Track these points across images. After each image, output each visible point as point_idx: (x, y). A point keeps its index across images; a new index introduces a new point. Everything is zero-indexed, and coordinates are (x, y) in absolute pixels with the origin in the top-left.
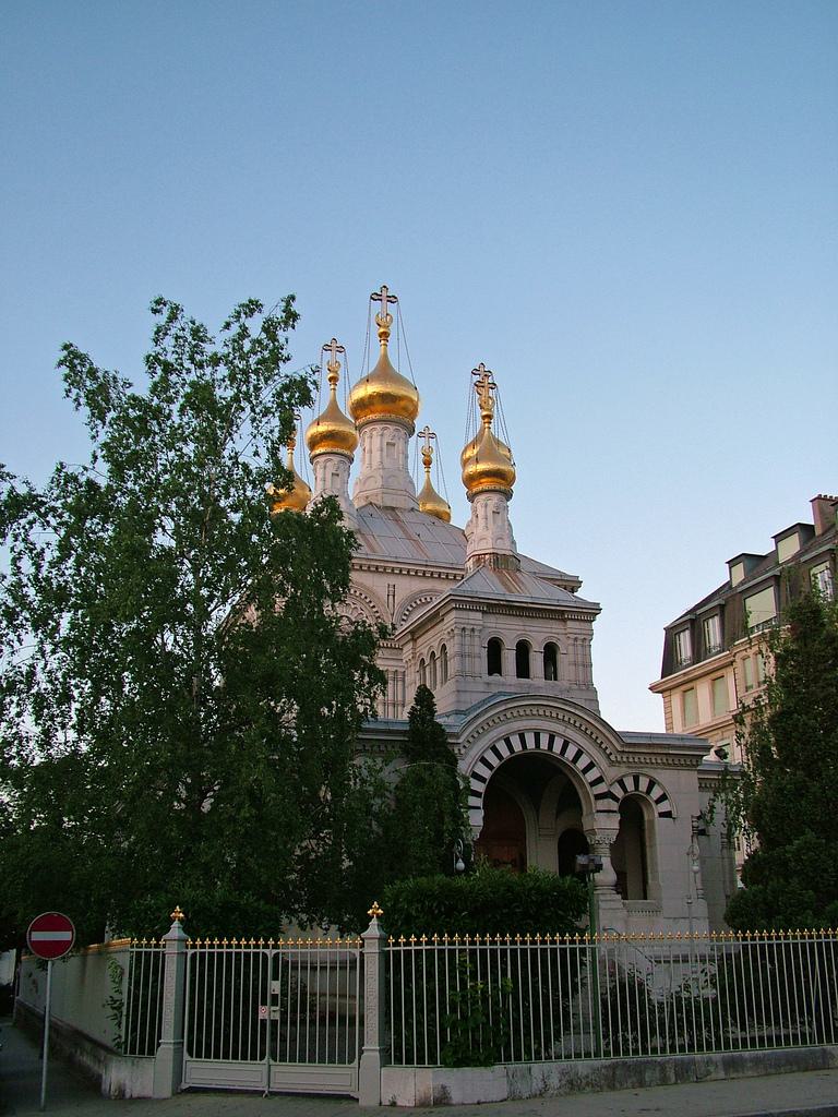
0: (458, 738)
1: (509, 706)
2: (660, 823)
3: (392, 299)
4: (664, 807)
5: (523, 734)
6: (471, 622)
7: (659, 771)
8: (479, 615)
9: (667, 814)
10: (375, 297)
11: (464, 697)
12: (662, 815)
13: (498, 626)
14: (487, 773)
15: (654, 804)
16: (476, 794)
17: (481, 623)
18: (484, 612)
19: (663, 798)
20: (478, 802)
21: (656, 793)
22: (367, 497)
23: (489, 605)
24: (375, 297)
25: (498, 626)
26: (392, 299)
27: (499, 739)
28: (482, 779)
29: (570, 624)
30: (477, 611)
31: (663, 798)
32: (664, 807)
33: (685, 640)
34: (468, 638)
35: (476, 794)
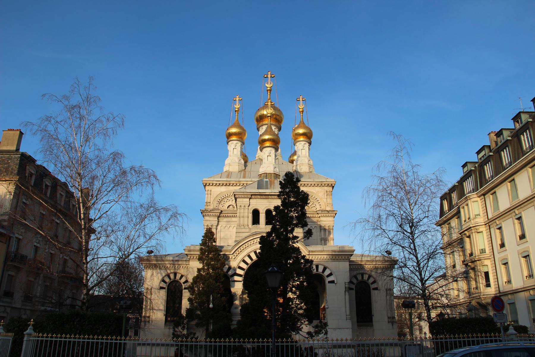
0: (230, 251)
1: (254, 237)
2: (328, 286)
4: (331, 278)
6: (244, 203)
7: (329, 262)
9: (332, 282)
11: (239, 234)
12: (330, 282)
13: (257, 203)
14: (245, 266)
15: (326, 277)
16: (240, 275)
19: (331, 274)
20: (240, 279)
21: (327, 272)
25: (257, 203)
28: (242, 269)
31: (331, 274)
32: (331, 278)
33: (445, 203)
34: (242, 210)
35: (240, 275)
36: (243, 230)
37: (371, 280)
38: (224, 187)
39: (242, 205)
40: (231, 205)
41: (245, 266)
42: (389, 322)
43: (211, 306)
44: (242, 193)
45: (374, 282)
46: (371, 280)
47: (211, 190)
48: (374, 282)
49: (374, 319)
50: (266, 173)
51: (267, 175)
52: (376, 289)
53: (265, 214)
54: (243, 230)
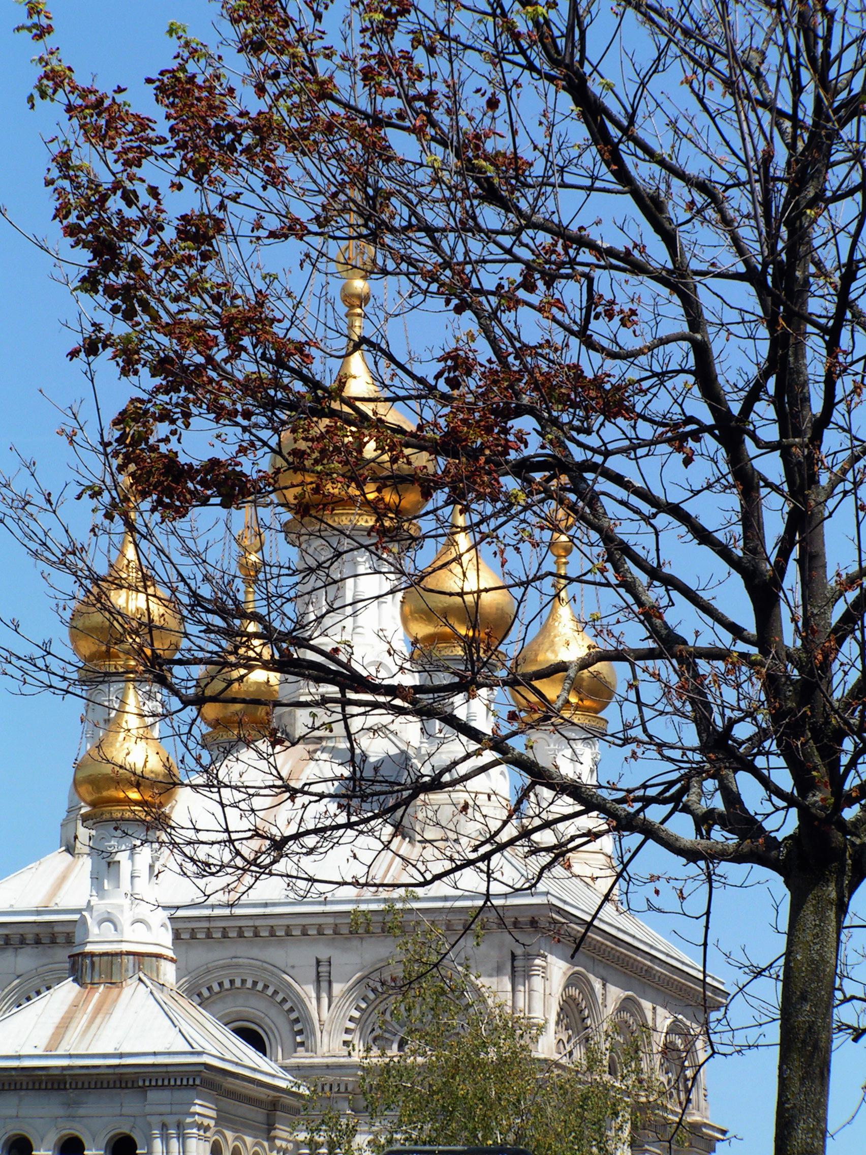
29: (152, 1095)
50: (92, 955)
51: (93, 963)
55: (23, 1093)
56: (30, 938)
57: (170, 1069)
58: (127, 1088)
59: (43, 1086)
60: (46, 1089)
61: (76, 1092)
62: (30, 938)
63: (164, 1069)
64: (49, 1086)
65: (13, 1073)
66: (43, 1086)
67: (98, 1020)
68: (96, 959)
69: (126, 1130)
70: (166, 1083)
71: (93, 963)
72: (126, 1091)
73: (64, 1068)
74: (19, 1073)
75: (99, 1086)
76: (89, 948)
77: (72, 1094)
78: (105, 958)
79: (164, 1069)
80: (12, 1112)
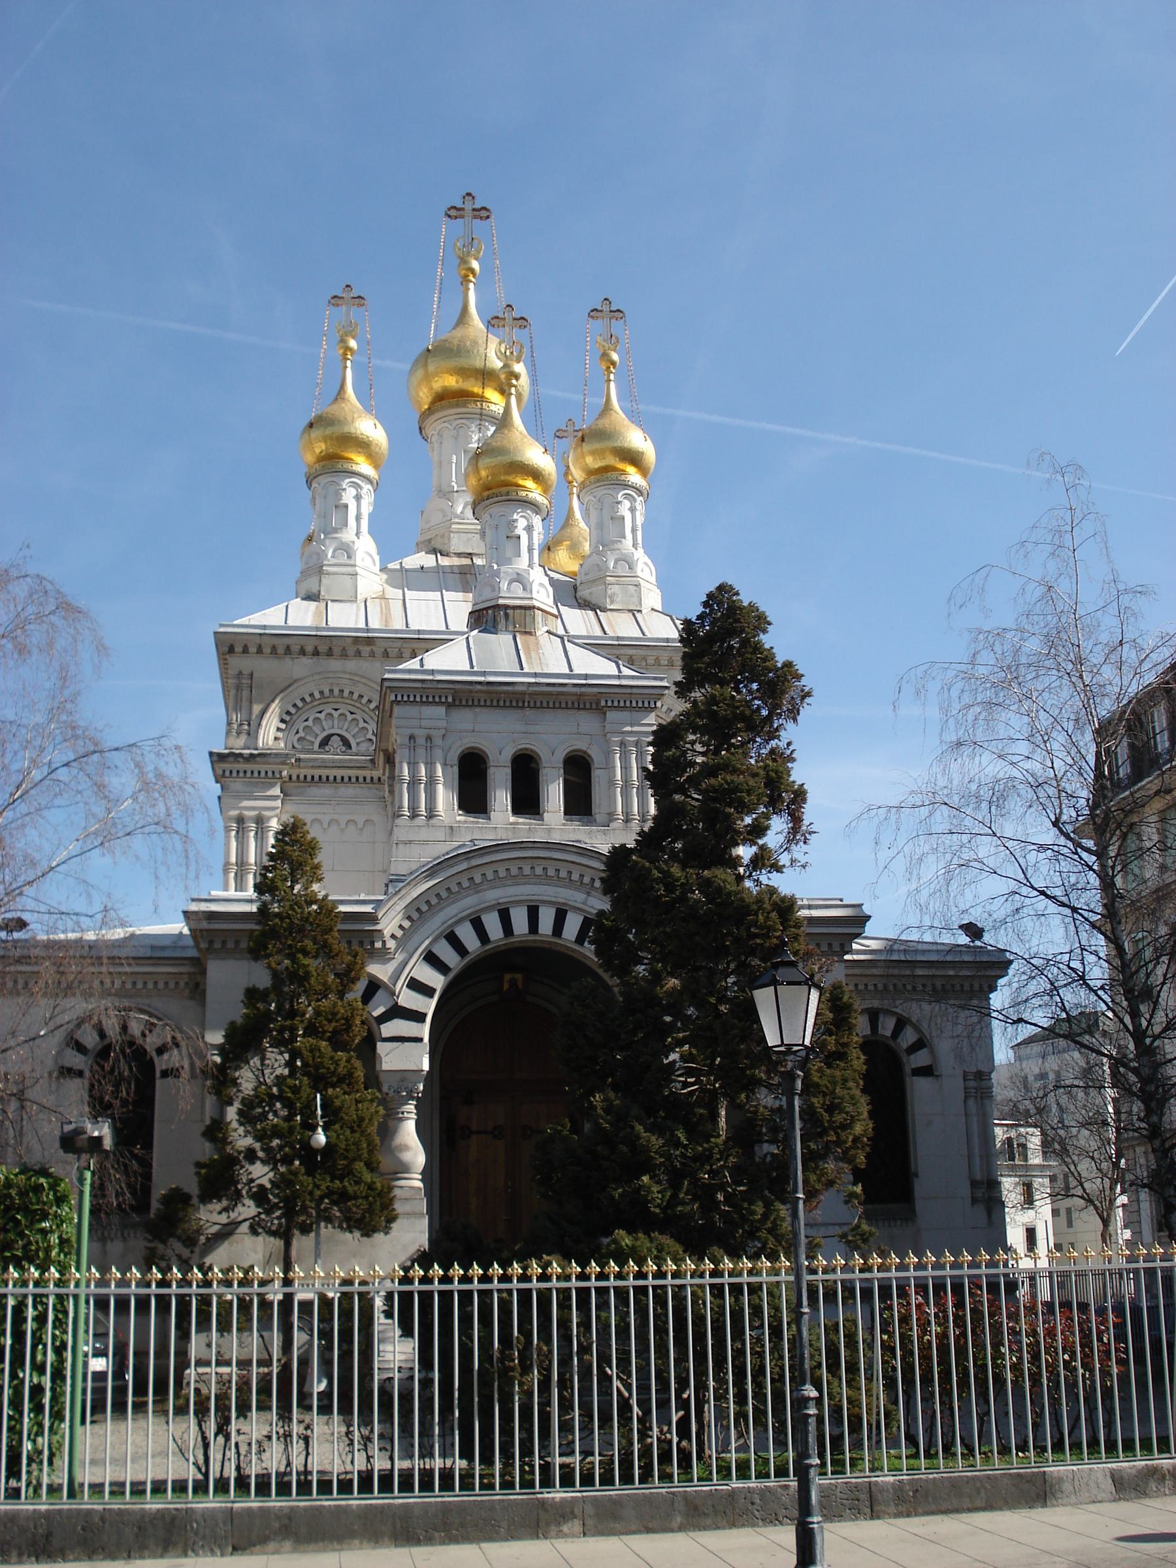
1: (474, 862)
3: (483, 213)
5: (507, 910)
6: (424, 723)
8: (441, 710)
10: (454, 213)
14: (437, 981)
16: (419, 1017)
17: (443, 724)
18: (449, 706)
22: (430, 541)
23: (455, 693)
24: (454, 213)
26: (483, 213)
27: (459, 921)
29: (611, 715)
30: (434, 703)
35: (419, 1017)
36: (424, 834)
37: (909, 1037)
38: (305, 660)
39: (416, 732)
40: (333, 735)
41: (437, 981)
42: (974, 1200)
43: (321, 1138)
44: (419, 685)
45: (919, 1045)
46: (909, 1037)
47: (252, 675)
48: (919, 1045)
49: (921, 1188)
50: (506, 607)
51: (507, 615)
52: (927, 1071)
53: (509, 771)
54: (424, 834)
55: (478, 710)
56: (309, 649)
57: (635, 691)
58: (585, 709)
59: (502, 703)
60: (504, 706)
61: (533, 711)
62: (309, 649)
63: (629, 691)
64: (508, 704)
65: (479, 687)
66: (502, 703)
67: (533, 655)
68: (510, 611)
69: (581, 745)
70: (628, 704)
71: (507, 615)
72: (581, 712)
73: (529, 684)
74: (485, 688)
75: (557, 705)
76: (501, 602)
77: (528, 712)
78: (518, 611)
79: (629, 691)
80: (469, 726)
